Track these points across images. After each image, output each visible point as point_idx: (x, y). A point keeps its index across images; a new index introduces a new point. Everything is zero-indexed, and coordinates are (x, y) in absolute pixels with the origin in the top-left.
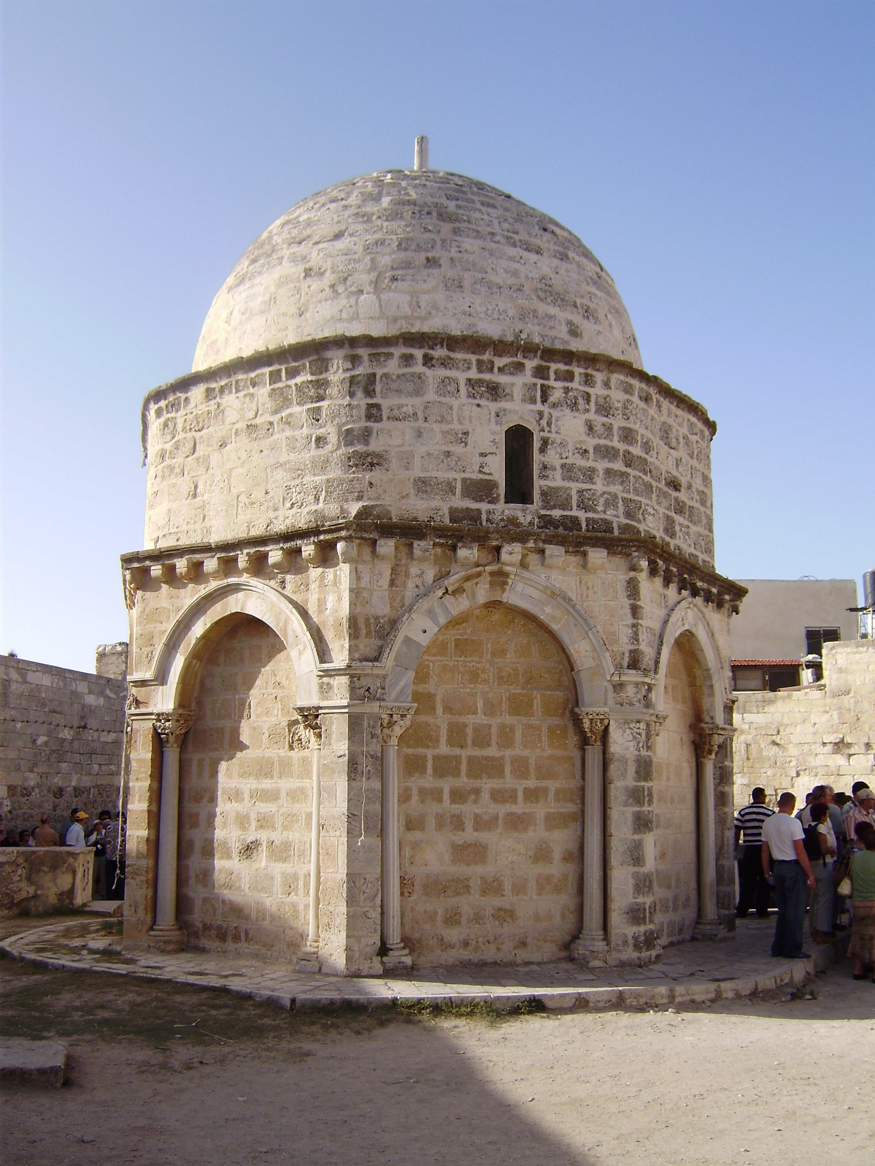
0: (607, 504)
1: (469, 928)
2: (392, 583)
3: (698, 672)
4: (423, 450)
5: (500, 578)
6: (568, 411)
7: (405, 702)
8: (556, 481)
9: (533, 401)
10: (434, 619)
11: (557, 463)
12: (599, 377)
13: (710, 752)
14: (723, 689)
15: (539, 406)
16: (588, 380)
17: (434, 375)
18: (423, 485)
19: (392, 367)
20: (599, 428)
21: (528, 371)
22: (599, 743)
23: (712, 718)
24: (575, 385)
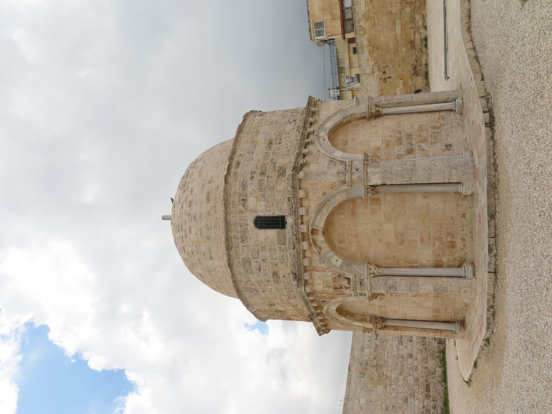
1: (457, 238)
3: (345, 121)
7: (365, 268)
10: (332, 257)
13: (379, 111)
14: (352, 107)
22: (377, 188)
23: (364, 113)
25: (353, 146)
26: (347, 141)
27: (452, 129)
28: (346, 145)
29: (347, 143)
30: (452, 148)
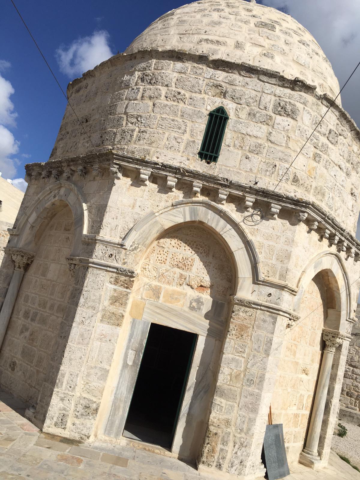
25: (60, 239)
26: (69, 230)
27: (29, 384)
28: (66, 230)
29: (67, 230)
30: (10, 369)
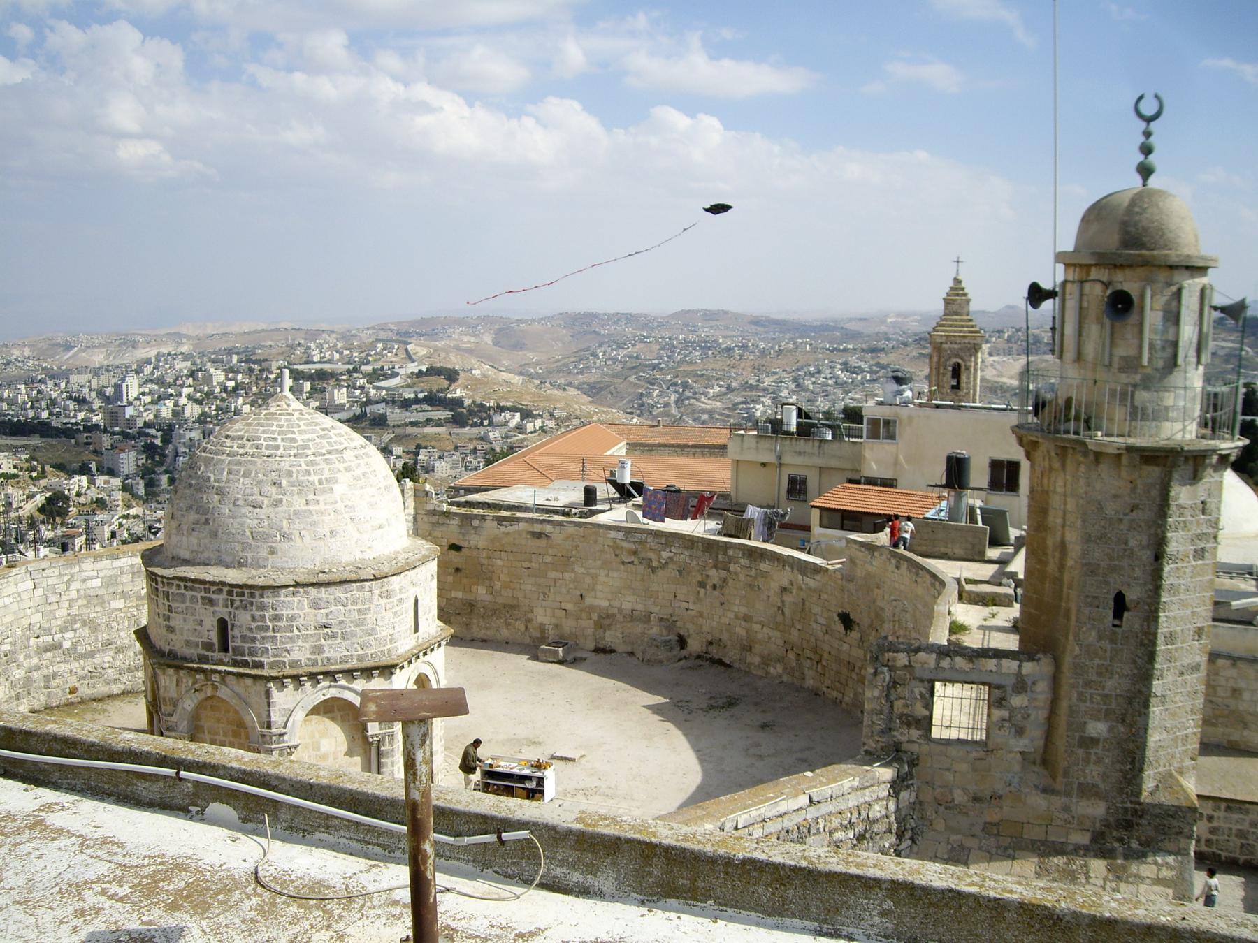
0: (263, 652)
2: (177, 685)
4: (186, 628)
5: (215, 688)
6: (243, 611)
8: (238, 643)
9: (227, 607)
11: (239, 635)
12: (257, 593)
15: (230, 609)
16: (252, 595)
17: (189, 594)
18: (188, 643)
19: (174, 589)
20: (258, 618)
21: (225, 593)
24: (245, 598)
